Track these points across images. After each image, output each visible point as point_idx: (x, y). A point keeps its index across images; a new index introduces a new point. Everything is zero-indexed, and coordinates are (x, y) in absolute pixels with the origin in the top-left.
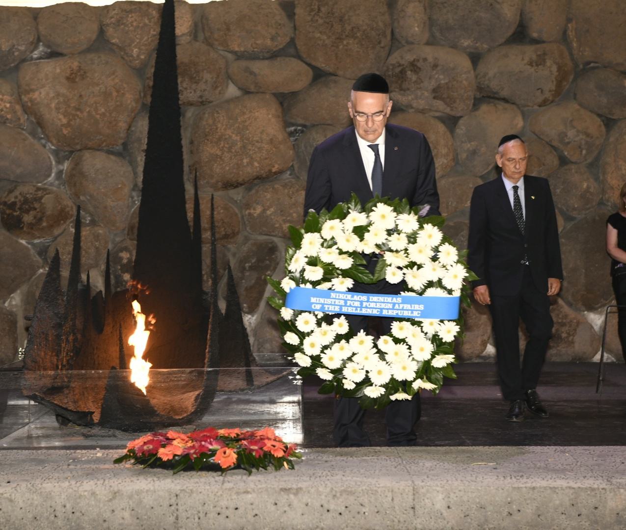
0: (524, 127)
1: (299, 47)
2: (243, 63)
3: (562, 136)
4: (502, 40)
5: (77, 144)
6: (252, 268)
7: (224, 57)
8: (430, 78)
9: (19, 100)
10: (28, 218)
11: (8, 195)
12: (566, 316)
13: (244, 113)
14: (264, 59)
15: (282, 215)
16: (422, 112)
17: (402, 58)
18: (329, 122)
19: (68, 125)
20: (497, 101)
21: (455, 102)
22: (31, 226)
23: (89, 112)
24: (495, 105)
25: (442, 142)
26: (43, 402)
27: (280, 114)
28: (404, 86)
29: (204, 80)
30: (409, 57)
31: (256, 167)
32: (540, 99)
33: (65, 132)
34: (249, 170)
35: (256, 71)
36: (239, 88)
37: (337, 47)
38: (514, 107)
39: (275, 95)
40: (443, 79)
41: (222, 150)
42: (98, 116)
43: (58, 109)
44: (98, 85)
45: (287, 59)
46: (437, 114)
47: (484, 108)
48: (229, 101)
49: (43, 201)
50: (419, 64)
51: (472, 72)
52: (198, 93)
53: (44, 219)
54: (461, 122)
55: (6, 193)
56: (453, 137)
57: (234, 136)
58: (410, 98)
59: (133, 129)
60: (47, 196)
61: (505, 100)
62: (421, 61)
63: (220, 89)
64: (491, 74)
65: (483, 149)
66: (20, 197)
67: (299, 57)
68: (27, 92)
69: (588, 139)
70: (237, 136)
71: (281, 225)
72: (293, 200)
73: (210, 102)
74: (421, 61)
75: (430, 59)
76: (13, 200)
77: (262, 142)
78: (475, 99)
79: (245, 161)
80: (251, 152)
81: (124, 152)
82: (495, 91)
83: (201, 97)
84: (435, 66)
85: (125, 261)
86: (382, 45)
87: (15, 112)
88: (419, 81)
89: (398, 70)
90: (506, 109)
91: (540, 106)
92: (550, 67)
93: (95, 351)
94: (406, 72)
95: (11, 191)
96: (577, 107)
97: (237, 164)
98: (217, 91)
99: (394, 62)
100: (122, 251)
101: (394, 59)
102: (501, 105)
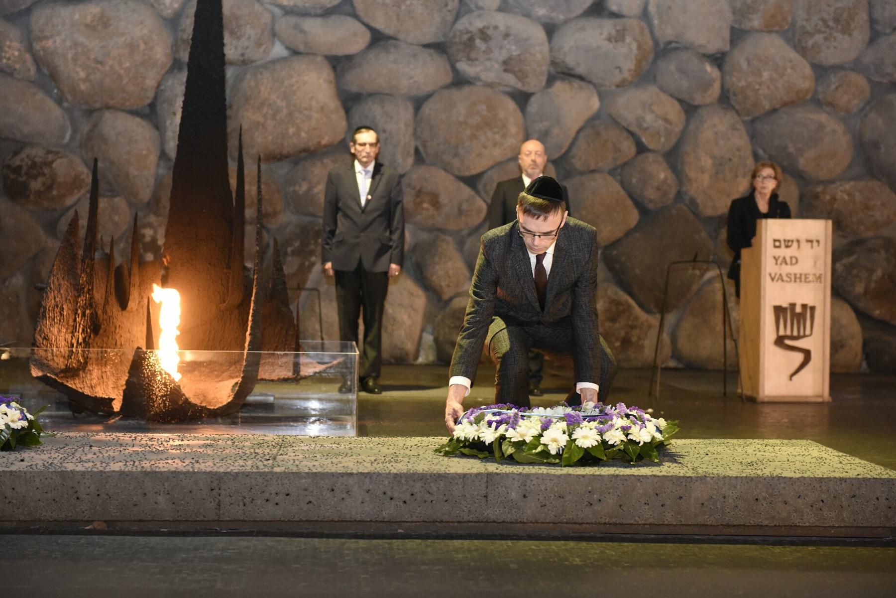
0: (600, 109)
2: (292, 20)
3: (640, 120)
4: (579, 11)
6: (294, 253)
7: (270, 12)
8: (501, 48)
9: (30, 49)
10: (36, 185)
11: (13, 157)
12: (637, 318)
13: (291, 77)
14: (317, 16)
16: (490, 85)
17: (470, 23)
18: (387, 91)
19: (87, 79)
21: (527, 77)
22: (39, 193)
24: (570, 83)
25: (511, 120)
27: (333, 80)
28: (473, 55)
29: (247, 36)
30: (479, 24)
33: (83, 87)
34: (295, 141)
36: (288, 48)
37: (399, 7)
38: (591, 87)
40: (515, 51)
41: (265, 116)
42: (122, 72)
43: (75, 60)
44: (123, 35)
45: (343, 18)
47: (559, 86)
48: (273, 62)
49: (54, 165)
51: (547, 44)
52: (240, 51)
53: (55, 186)
54: (533, 99)
55: (11, 155)
58: (478, 69)
60: (59, 161)
61: (581, 78)
62: (491, 28)
63: (264, 47)
64: (566, 48)
66: (26, 160)
67: (355, 16)
68: (40, 39)
69: (668, 126)
74: (491, 28)
75: (502, 28)
76: (18, 163)
79: (291, 130)
81: (150, 113)
82: (570, 66)
83: (243, 55)
84: (507, 35)
85: (148, 239)
86: (449, 8)
87: (25, 62)
88: (489, 51)
89: (466, 37)
92: (630, 44)
93: (117, 331)
95: (16, 153)
96: (657, 90)
98: (262, 49)
101: (462, 24)
102: (577, 84)
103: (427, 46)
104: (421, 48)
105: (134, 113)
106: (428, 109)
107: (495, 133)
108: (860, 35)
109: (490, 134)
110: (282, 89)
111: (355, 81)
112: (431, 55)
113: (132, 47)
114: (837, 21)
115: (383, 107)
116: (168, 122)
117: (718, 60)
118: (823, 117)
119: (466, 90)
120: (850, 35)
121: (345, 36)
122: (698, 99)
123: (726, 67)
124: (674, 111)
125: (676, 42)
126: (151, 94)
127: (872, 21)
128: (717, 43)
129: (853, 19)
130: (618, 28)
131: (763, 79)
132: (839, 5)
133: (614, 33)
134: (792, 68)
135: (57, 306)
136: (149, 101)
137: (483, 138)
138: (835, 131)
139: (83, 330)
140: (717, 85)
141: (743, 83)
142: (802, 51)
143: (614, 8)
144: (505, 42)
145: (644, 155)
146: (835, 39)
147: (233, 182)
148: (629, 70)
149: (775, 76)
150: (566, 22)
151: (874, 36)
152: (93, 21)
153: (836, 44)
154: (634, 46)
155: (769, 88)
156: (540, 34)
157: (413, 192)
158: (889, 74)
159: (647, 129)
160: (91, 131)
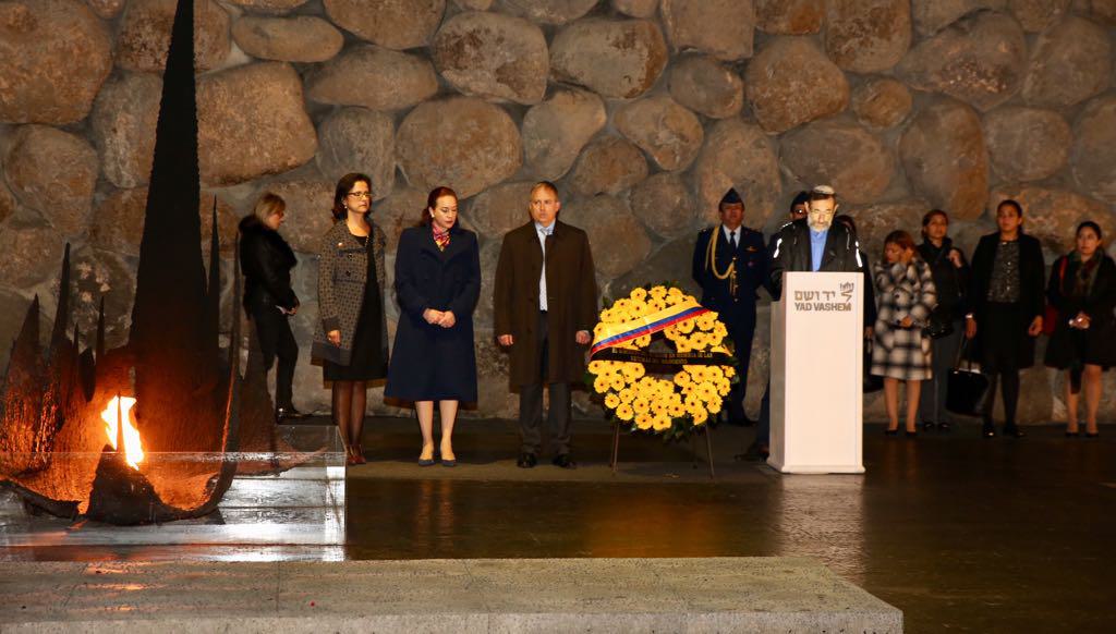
0: (607, 122)
1: (326, 5)
2: (253, 22)
3: (652, 137)
4: (584, 12)
5: (22, 116)
8: (494, 55)
13: (252, 88)
14: (280, 16)
15: (298, 223)
16: (482, 97)
17: (459, 27)
18: (363, 104)
19: (10, 90)
20: (575, 89)
21: (523, 87)
23: (40, 74)
25: (506, 137)
26: (18, 490)
27: (300, 91)
28: (462, 62)
29: (200, 41)
30: (468, 27)
31: (267, 159)
32: (627, 90)
34: (257, 161)
35: (270, 33)
36: (246, 53)
37: (377, 7)
39: (293, 64)
41: (221, 134)
44: (53, 38)
46: (501, 101)
47: (559, 96)
50: (479, 37)
51: (546, 50)
54: (530, 112)
56: (520, 130)
57: (238, 116)
58: (468, 79)
59: (101, 99)
61: (585, 88)
62: (483, 32)
63: (220, 52)
64: (568, 54)
65: (557, 149)
69: (684, 143)
70: (241, 116)
71: (296, 235)
72: (314, 203)
73: (206, 70)
74: (483, 32)
75: (494, 30)
77: (275, 127)
78: (548, 85)
79: (252, 150)
80: (260, 139)
82: (572, 75)
84: (500, 40)
85: (84, 276)
86: (434, 8)
88: (479, 58)
89: (453, 42)
90: (585, 99)
91: (627, 97)
92: (640, 50)
94: (463, 45)
96: (671, 101)
97: (241, 153)
98: (217, 56)
99: (448, 31)
100: (81, 263)
101: (447, 29)
102: (581, 94)
103: (409, 52)
104: (403, 55)
105: (68, 129)
106: (410, 124)
107: (487, 152)
108: (899, 39)
109: (481, 153)
110: (242, 102)
111: (323, 94)
112: (413, 63)
113: (65, 54)
114: (874, 23)
115: (359, 122)
116: (108, 141)
117: (740, 68)
118: (858, 134)
119: (454, 102)
120: (889, 39)
121: (313, 40)
122: (717, 113)
123: (750, 77)
124: (690, 124)
125: (694, 47)
126: (86, 108)
127: (914, 23)
128: (737, 51)
129: (892, 22)
130: (627, 32)
131: (791, 90)
132: (876, 5)
133: (622, 37)
134: (824, 77)
135: (16, 401)
136: (82, 116)
137: (474, 158)
138: (872, 149)
139: (47, 428)
140: (739, 97)
141: (768, 95)
142: (837, 58)
143: (623, 9)
144: (499, 48)
145: (658, 176)
146: (872, 43)
147: (207, 262)
148: (640, 80)
149: (804, 86)
150: (567, 24)
151: (916, 41)
152: (16, 21)
153: (873, 50)
154: (645, 52)
155: (797, 100)
156: (536, 39)
157: (393, 220)
158: (932, 84)
159: (660, 146)
160: (16, 149)
